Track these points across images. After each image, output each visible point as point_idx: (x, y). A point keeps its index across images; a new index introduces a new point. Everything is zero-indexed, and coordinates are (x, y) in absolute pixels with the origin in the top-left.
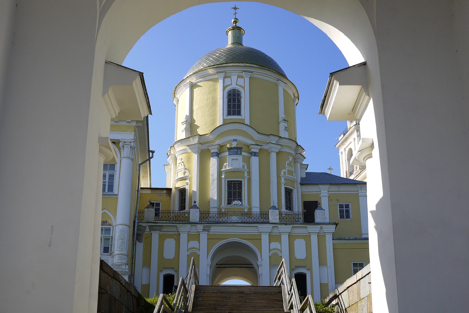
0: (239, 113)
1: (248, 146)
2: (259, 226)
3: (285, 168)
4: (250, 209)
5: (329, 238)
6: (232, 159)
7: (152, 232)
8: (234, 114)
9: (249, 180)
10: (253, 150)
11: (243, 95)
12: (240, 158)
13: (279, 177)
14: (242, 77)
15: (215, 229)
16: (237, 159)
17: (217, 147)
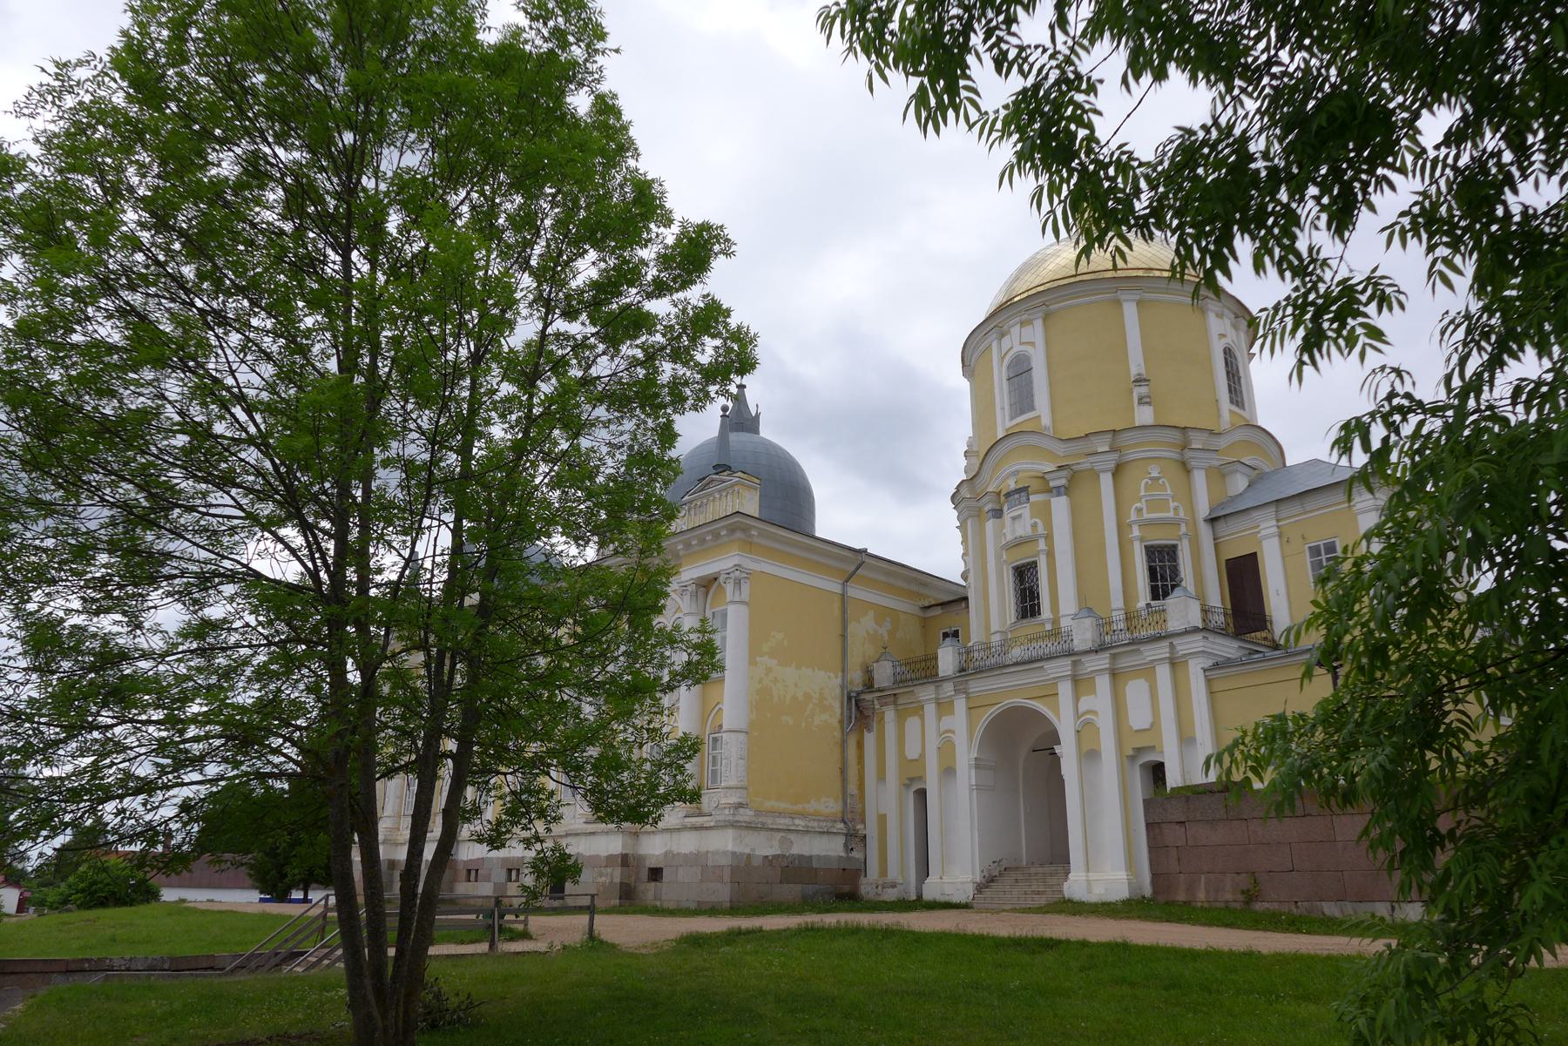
0: (1032, 408)
1: (1043, 478)
2: (1047, 665)
3: (1140, 500)
4: (1056, 621)
5: (1195, 669)
6: (1014, 518)
7: (884, 708)
8: (1022, 412)
9: (1050, 554)
10: (1052, 484)
11: (1034, 364)
12: (1025, 511)
13: (1122, 528)
14: (1030, 322)
15: (978, 686)
16: (1020, 516)
17: (986, 499)
